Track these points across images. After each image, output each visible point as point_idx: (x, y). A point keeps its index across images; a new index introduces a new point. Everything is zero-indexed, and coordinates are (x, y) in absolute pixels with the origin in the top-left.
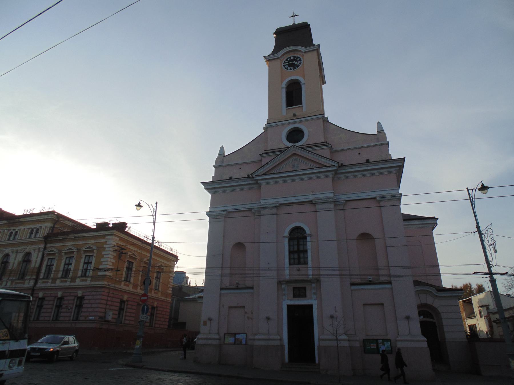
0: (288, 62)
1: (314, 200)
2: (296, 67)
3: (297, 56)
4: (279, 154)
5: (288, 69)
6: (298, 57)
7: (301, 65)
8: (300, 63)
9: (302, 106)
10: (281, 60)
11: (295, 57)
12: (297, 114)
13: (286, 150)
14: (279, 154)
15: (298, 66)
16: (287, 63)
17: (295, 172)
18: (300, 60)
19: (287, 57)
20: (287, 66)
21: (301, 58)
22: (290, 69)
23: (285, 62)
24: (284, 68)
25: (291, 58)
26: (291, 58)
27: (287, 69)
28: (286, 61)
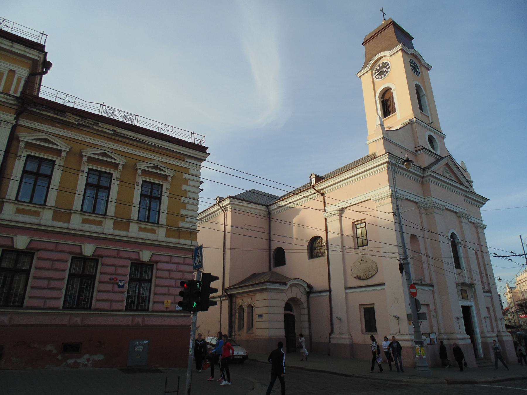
0: (378, 72)
2: (385, 73)
3: (384, 61)
5: (379, 78)
6: (386, 63)
8: (389, 68)
11: (383, 63)
15: (387, 72)
16: (377, 73)
18: (388, 64)
21: (388, 62)
25: (380, 66)
26: (380, 65)
27: (378, 79)
28: (376, 71)
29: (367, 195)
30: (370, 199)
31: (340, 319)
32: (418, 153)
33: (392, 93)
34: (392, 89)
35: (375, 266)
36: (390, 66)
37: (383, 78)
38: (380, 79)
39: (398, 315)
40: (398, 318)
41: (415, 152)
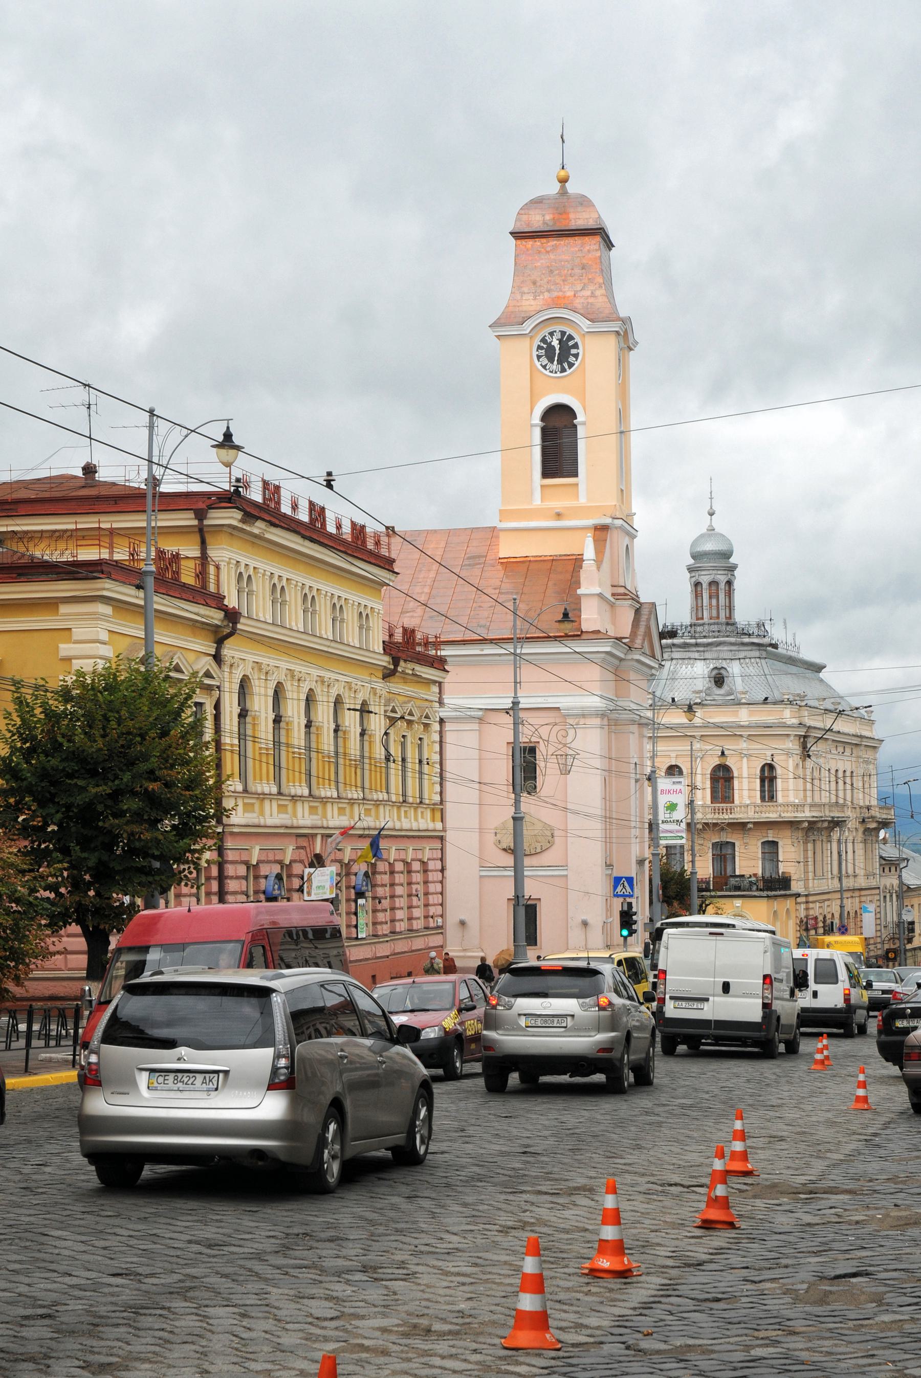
2: (566, 365)
3: (569, 331)
6: (571, 338)
7: (577, 364)
9: (577, 485)
10: (531, 337)
18: (576, 346)
19: (545, 332)
20: (545, 361)
21: (578, 339)
23: (539, 348)
24: (538, 364)
27: (544, 367)
29: (550, 700)
30: (558, 709)
31: (463, 923)
32: (618, 602)
33: (575, 426)
34: (576, 418)
35: (549, 834)
36: (580, 351)
37: (559, 374)
39: (590, 921)
40: (585, 924)
41: (612, 599)
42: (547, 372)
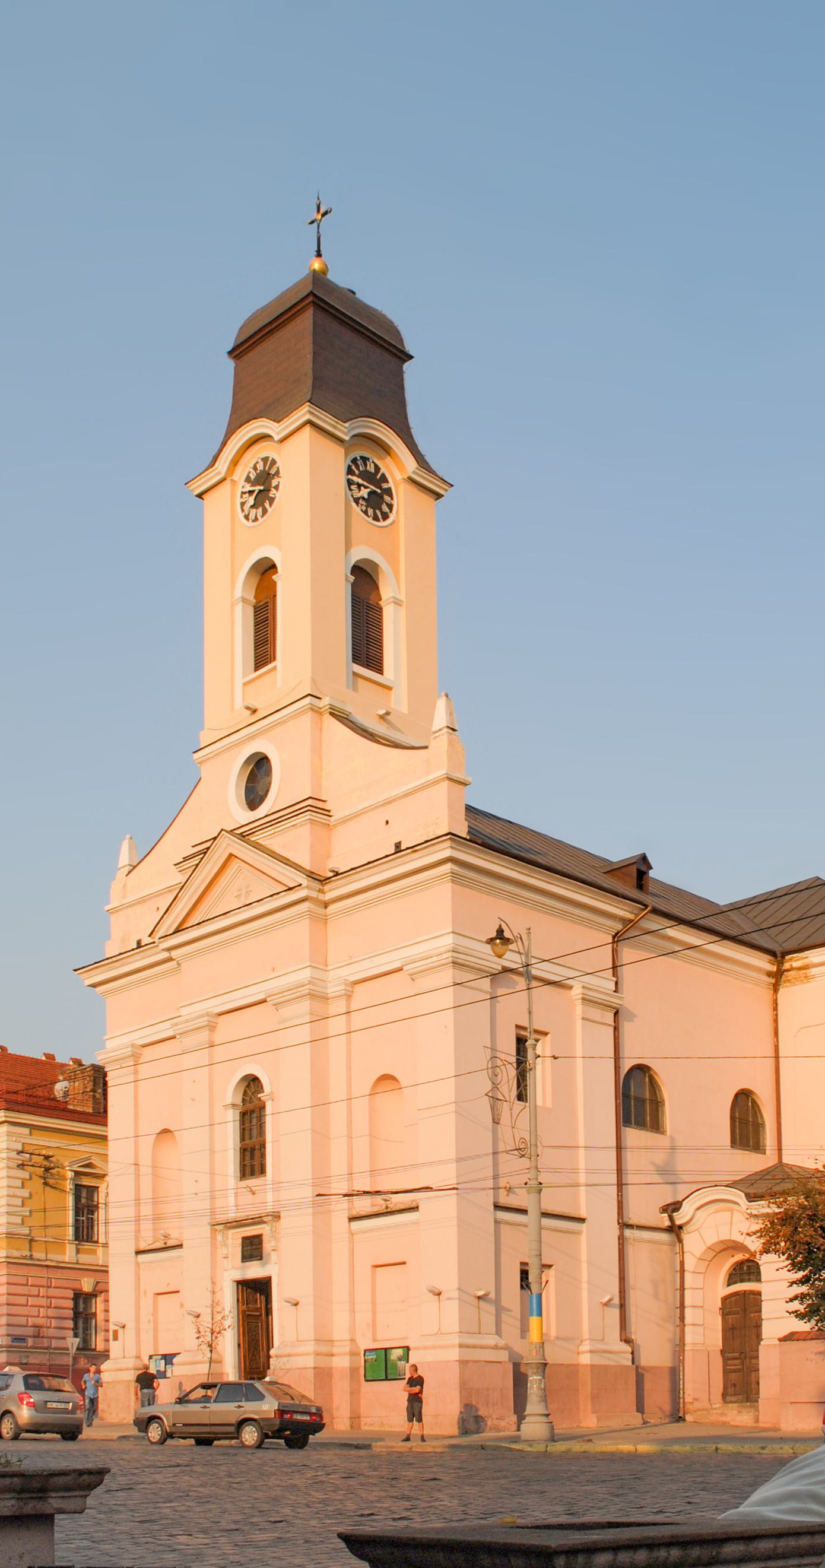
1: (270, 996)
4: (197, 865)
12: (254, 704)
13: (208, 848)
14: (197, 865)
17: (231, 916)
22: (253, 518)
24: (241, 516)
38: (253, 521)
42: (250, 524)
